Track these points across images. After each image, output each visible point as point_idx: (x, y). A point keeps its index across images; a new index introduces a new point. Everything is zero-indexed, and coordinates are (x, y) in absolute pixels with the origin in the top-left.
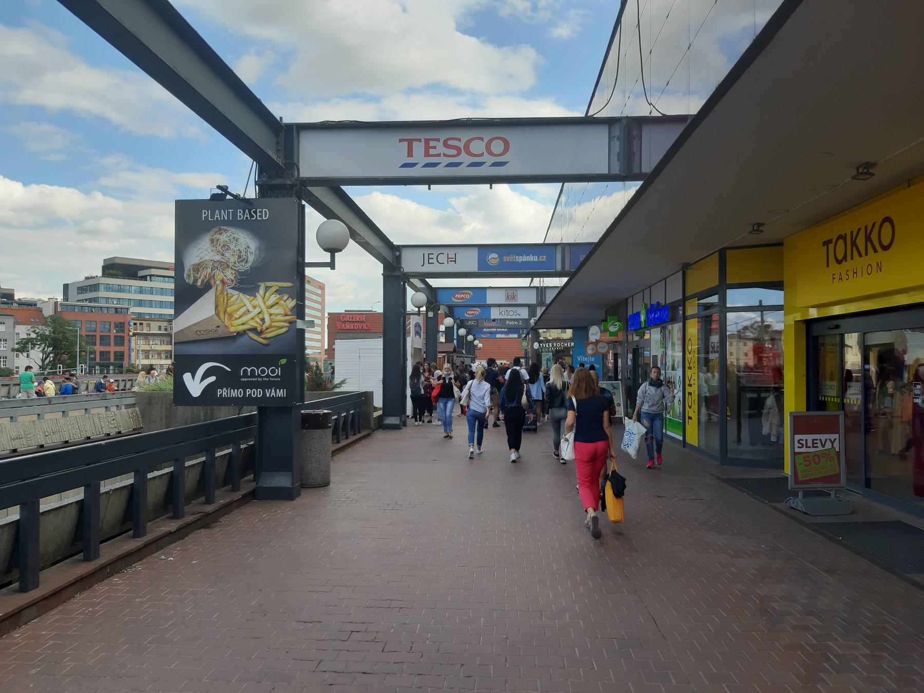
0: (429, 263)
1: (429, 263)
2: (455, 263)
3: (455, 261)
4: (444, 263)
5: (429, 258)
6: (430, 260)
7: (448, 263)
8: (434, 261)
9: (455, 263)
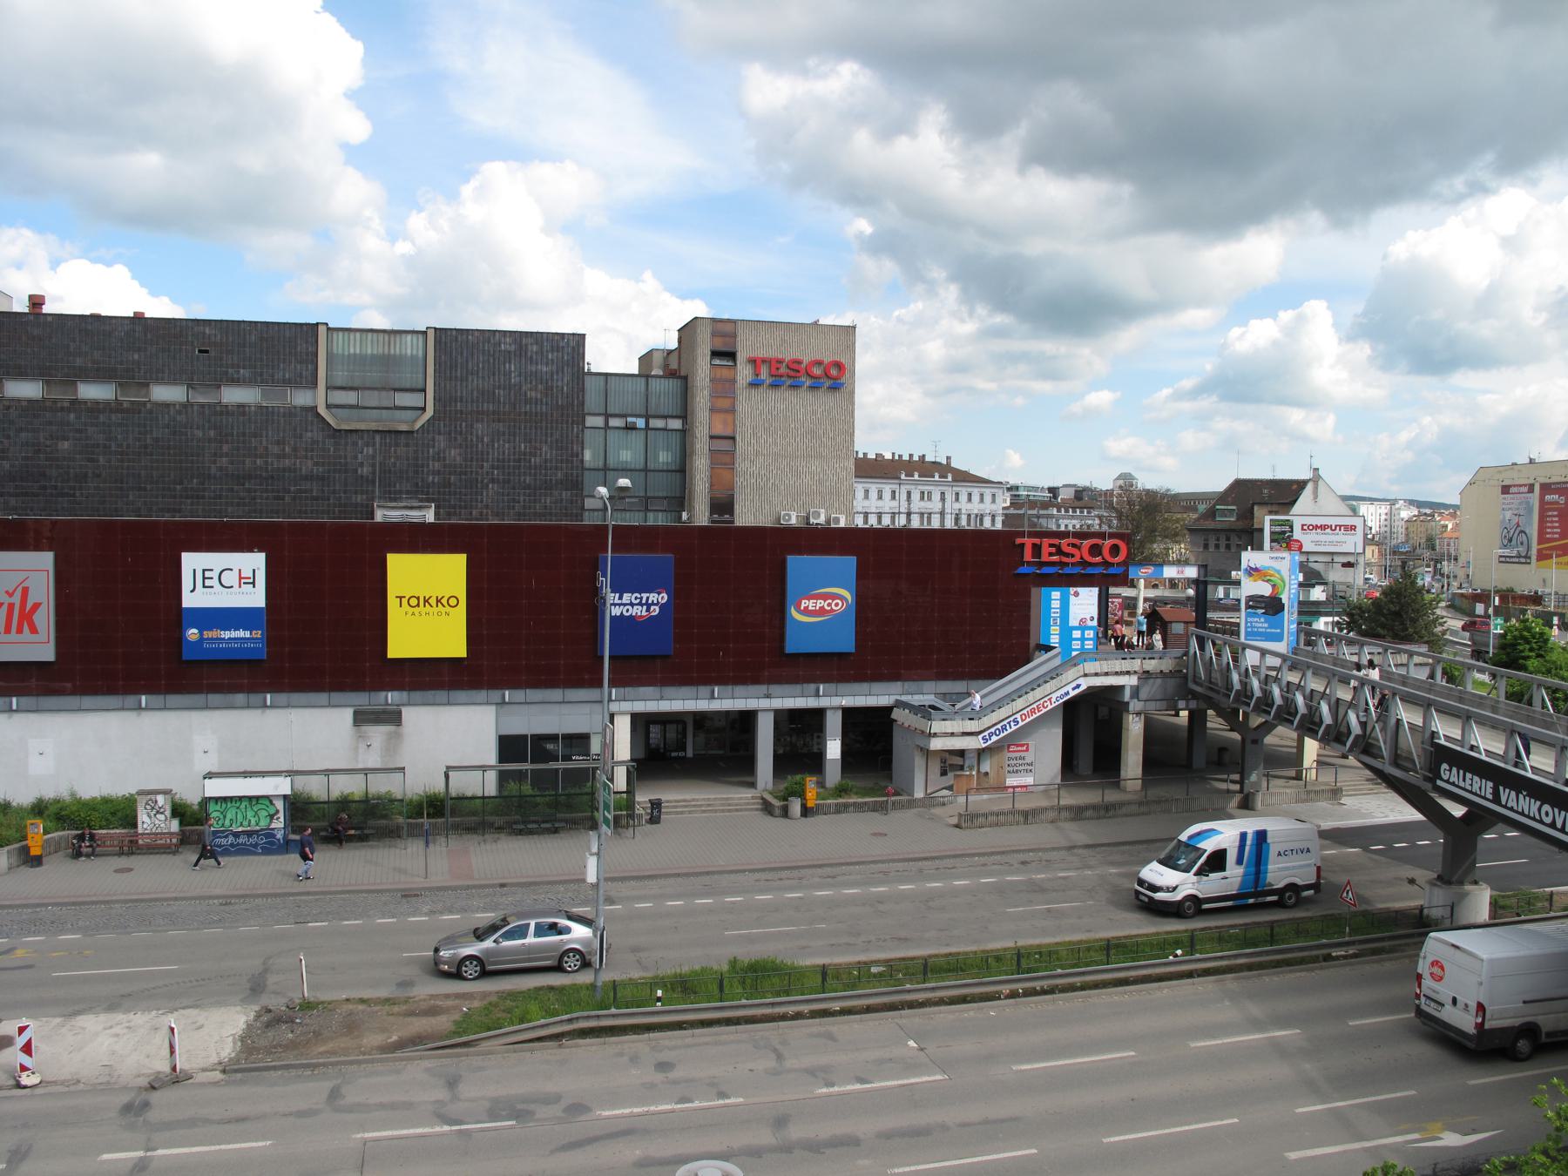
0: (204, 586)
1: (204, 586)
2: (254, 587)
3: (253, 583)
4: (232, 587)
5: (204, 578)
6: (206, 581)
7: (240, 586)
8: (215, 582)
9: (254, 587)
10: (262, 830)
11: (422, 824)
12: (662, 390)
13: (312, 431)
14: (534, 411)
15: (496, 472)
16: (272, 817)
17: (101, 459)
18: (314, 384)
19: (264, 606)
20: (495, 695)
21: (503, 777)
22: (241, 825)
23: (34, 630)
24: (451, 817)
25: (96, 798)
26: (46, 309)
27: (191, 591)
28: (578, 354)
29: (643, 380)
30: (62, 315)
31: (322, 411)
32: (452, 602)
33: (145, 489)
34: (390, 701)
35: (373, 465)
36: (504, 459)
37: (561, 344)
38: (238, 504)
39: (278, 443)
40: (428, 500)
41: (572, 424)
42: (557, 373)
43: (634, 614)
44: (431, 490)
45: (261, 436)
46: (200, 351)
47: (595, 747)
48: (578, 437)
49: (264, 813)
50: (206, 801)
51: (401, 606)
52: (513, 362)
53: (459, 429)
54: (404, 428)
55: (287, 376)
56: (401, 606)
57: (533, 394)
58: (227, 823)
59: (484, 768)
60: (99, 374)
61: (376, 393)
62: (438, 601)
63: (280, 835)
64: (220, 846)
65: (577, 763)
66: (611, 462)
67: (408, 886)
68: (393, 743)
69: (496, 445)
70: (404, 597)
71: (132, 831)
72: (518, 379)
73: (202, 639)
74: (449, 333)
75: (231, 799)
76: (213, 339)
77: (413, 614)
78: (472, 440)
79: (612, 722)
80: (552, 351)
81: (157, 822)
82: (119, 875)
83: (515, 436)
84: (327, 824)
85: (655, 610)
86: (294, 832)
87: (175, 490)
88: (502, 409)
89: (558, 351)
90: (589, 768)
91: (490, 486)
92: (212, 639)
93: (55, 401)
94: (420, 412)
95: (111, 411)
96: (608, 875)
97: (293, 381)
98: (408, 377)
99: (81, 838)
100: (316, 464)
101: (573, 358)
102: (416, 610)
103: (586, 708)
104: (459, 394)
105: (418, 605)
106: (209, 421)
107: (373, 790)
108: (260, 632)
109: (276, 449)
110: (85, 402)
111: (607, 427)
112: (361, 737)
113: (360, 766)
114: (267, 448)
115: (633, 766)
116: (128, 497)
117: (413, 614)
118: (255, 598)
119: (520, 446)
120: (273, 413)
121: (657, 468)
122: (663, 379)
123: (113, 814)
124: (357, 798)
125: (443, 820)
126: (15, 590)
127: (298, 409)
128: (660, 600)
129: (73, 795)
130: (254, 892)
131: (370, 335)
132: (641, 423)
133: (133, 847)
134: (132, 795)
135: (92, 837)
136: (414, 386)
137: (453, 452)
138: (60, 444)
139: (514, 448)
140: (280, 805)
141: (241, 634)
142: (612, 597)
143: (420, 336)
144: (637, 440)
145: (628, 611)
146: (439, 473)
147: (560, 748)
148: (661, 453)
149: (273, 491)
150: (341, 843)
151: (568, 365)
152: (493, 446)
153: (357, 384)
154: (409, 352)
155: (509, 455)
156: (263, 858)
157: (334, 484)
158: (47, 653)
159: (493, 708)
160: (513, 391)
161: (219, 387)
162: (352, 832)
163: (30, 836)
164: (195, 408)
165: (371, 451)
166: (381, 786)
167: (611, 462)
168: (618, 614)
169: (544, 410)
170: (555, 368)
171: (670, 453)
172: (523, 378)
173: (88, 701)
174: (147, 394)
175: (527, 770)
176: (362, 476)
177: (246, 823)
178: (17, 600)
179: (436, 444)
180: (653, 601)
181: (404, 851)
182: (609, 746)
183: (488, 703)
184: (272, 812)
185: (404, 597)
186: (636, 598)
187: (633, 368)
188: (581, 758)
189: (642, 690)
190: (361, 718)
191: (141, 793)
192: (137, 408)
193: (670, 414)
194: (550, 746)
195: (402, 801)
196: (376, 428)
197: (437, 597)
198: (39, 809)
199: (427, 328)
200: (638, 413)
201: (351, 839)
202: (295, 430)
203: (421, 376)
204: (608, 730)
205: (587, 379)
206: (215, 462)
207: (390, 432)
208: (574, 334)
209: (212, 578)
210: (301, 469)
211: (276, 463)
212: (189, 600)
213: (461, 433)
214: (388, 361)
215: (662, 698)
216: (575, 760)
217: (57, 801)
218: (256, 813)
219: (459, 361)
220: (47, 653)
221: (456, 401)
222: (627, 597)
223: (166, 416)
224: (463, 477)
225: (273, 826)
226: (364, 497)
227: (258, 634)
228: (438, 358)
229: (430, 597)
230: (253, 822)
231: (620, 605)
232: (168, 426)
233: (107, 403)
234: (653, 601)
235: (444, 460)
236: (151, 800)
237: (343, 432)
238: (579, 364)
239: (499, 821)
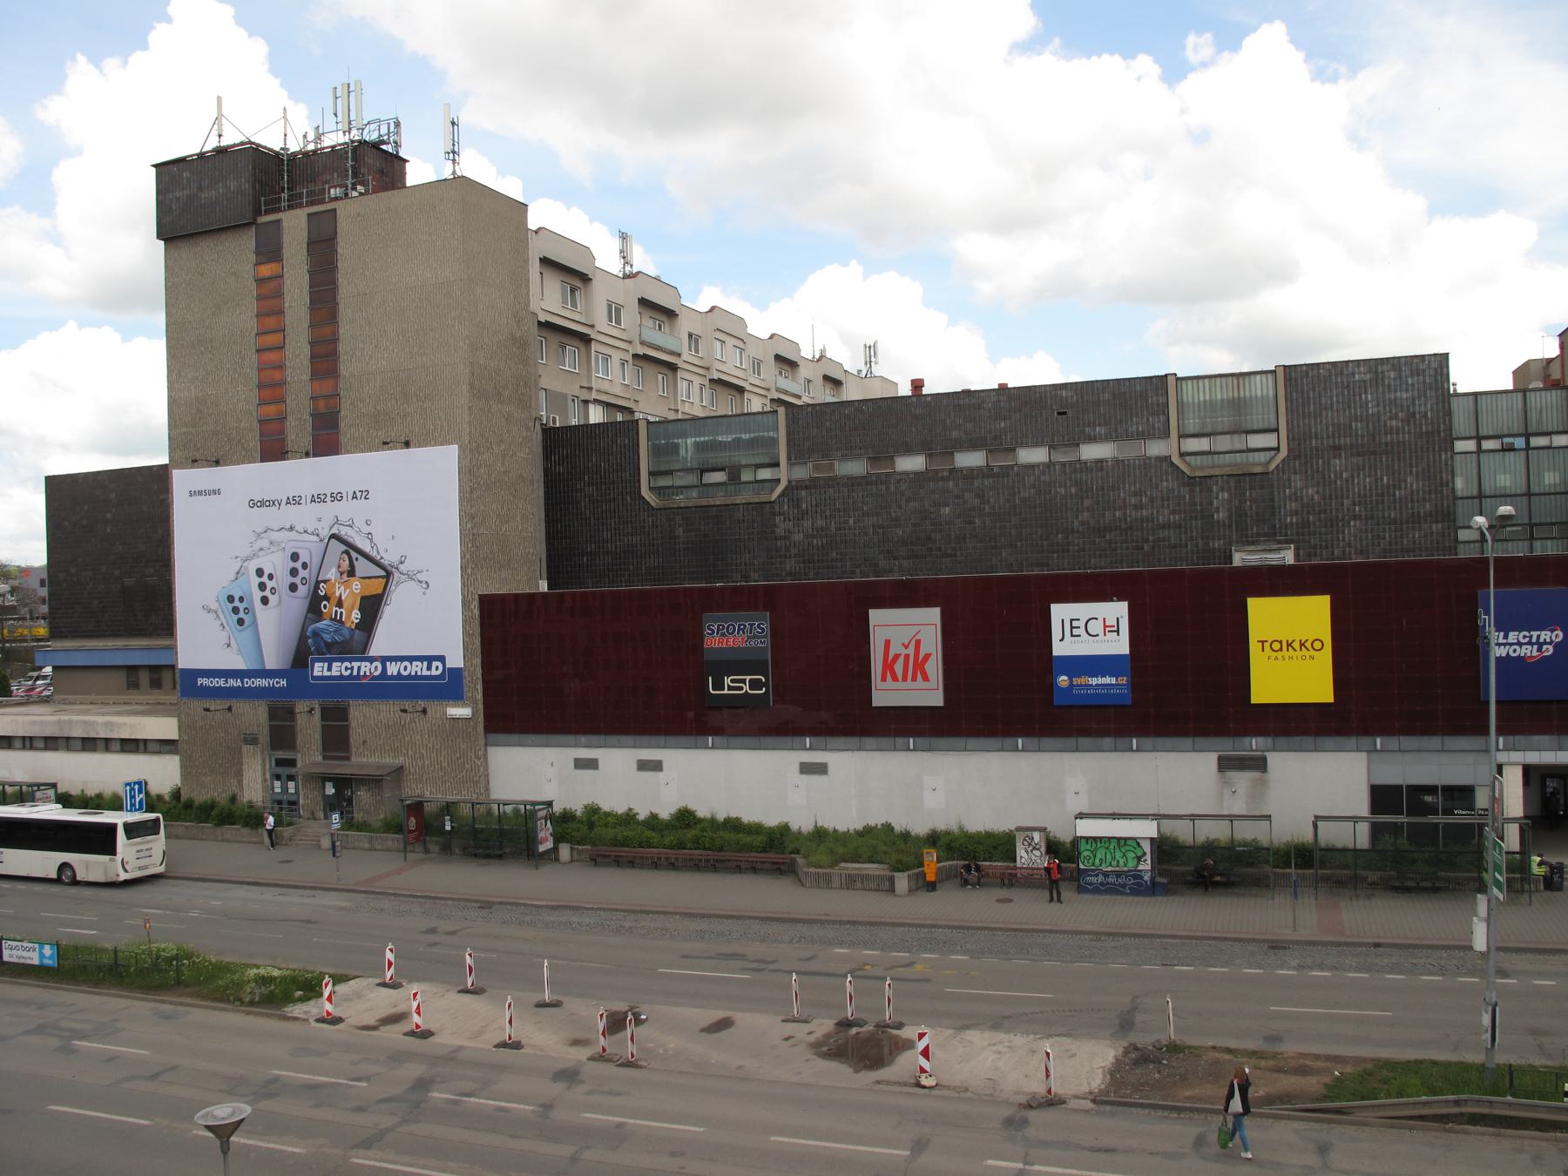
0: (1072, 635)
1: (1072, 635)
2: (1118, 635)
3: (1118, 631)
5: (1072, 628)
6: (1074, 630)
7: (1105, 635)
8: (1082, 631)
9: (1118, 635)
10: (1130, 871)
11: (1290, 875)
12: (1544, 405)
13: (1167, 481)
14: (1395, 440)
15: (1357, 508)
16: (1139, 859)
17: (977, 521)
18: (1166, 434)
19: (1128, 653)
20: (1365, 741)
21: (1377, 830)
22: (1110, 865)
23: (926, 678)
24: (1321, 868)
25: (981, 832)
26: (925, 391)
27: (1061, 640)
28: (1442, 375)
29: (1520, 395)
30: (939, 394)
31: (1176, 460)
32: (1317, 645)
33: (1016, 546)
34: (1254, 747)
35: (1229, 510)
36: (1365, 495)
37: (1421, 367)
38: (1101, 556)
39: (1135, 494)
40: (1287, 542)
41: (1440, 450)
42: (1419, 398)
43: (1522, 655)
44: (1289, 533)
45: (1119, 490)
46: (1059, 414)
47: (1482, 800)
48: (1447, 464)
49: (1131, 855)
50: (1076, 841)
51: (1263, 650)
52: (1369, 391)
53: (1315, 467)
54: (1258, 470)
55: (1140, 429)
56: (1263, 650)
57: (1394, 423)
58: (1097, 862)
59: (1355, 819)
60: (973, 446)
61: (1228, 436)
62: (1302, 645)
63: (1147, 877)
64: (1091, 884)
65: (1461, 817)
66: (1487, 490)
67: (1275, 938)
68: (1259, 791)
69: (1356, 481)
70: (1266, 641)
71: (1012, 865)
72: (1376, 409)
73: (1071, 686)
74: (1299, 369)
75: (1101, 838)
76: (1069, 400)
77: (1276, 658)
78: (1330, 477)
79: (1500, 773)
80: (1412, 375)
81: (1033, 857)
82: (1001, 905)
83: (1376, 469)
84: (1192, 868)
85: (1549, 650)
86: (1161, 875)
87: (1042, 545)
88: (1360, 442)
89: (1418, 375)
90: (1475, 823)
91: (1352, 523)
92: (1081, 685)
93: (936, 472)
94: (1273, 453)
95: (984, 477)
96: (1499, 945)
97: (1146, 434)
98: (1257, 420)
99: (968, 868)
100: (1174, 512)
101: (1436, 381)
102: (1279, 654)
103: (1470, 758)
104: (1313, 430)
105: (1281, 649)
106: (1070, 479)
107: (1239, 836)
108: (1125, 678)
109: (1133, 501)
110: (961, 470)
111: (1479, 450)
112: (1226, 783)
113: (1225, 812)
114: (1125, 500)
115: (1528, 824)
116: (1001, 554)
117: (1276, 658)
118: (1120, 645)
119: (1382, 480)
120: (1129, 465)
121: (1542, 491)
122: (1543, 393)
123: (995, 848)
124: (1222, 844)
125: (1311, 871)
126: (910, 642)
127: (1153, 460)
128: (1554, 638)
129: (961, 828)
130: (1123, 931)
131: (1218, 380)
132: (1519, 443)
133: (1012, 880)
134: (1011, 831)
135: (978, 869)
136: (1266, 426)
137: (1310, 491)
138: (942, 511)
139: (1376, 482)
140: (1147, 847)
141: (1108, 680)
142: (1495, 636)
143: (1270, 376)
144: (1515, 461)
145: (1515, 651)
146: (1296, 513)
147: (1440, 800)
148: (1546, 474)
149: (1132, 541)
150: (1206, 889)
151: (1431, 388)
152: (1354, 480)
153: (1208, 429)
154: (1259, 393)
155: (1371, 489)
156: (1130, 898)
157: (1192, 532)
158: (936, 698)
159: (1365, 754)
160: (1371, 424)
161: (1078, 445)
162: (1218, 878)
163: (926, 863)
164: (1057, 467)
165: (1226, 495)
166: (1247, 832)
167: (1488, 489)
168: (1504, 655)
169: (1407, 439)
170: (1416, 393)
171: (1557, 474)
172: (1381, 409)
173: (972, 742)
174: (1015, 458)
175: (1403, 823)
176: (1218, 522)
177: (1114, 863)
178: (911, 650)
179: (1293, 484)
180: (1545, 640)
181: (1271, 901)
182: (1496, 800)
183: (1358, 750)
184: (1140, 854)
185: (1266, 641)
186: (1524, 637)
187: (1507, 384)
188: (1464, 813)
189: (1536, 738)
190: (1225, 764)
191: (1019, 829)
192: (1006, 470)
193: (1555, 429)
194: (1429, 799)
195: (1268, 849)
196: (1230, 473)
197: (1301, 641)
198: (934, 839)
199: (1276, 367)
200: (1516, 432)
201: (1217, 884)
202: (1151, 480)
203: (1273, 416)
204: (1496, 783)
205: (1454, 401)
206: (1077, 518)
207: (1243, 475)
208: (1435, 355)
209: (1079, 627)
210: (1158, 518)
211: (1133, 513)
212: (1060, 648)
213: (1318, 471)
214: (1238, 405)
215: (1560, 749)
216: (1458, 815)
217: (948, 833)
218: (1124, 853)
219: (1312, 396)
220: (936, 698)
221: (1310, 439)
222: (1512, 636)
223: (1032, 478)
224: (1323, 516)
225: (1140, 868)
226: (1222, 542)
227: (1124, 680)
228: (1289, 395)
229: (1294, 641)
230: (1121, 863)
231: (1505, 645)
232: (1033, 486)
233: (980, 469)
234: (1545, 640)
235: (1302, 500)
236: (1028, 836)
237: (1197, 479)
238: (1443, 388)
239: (1373, 876)
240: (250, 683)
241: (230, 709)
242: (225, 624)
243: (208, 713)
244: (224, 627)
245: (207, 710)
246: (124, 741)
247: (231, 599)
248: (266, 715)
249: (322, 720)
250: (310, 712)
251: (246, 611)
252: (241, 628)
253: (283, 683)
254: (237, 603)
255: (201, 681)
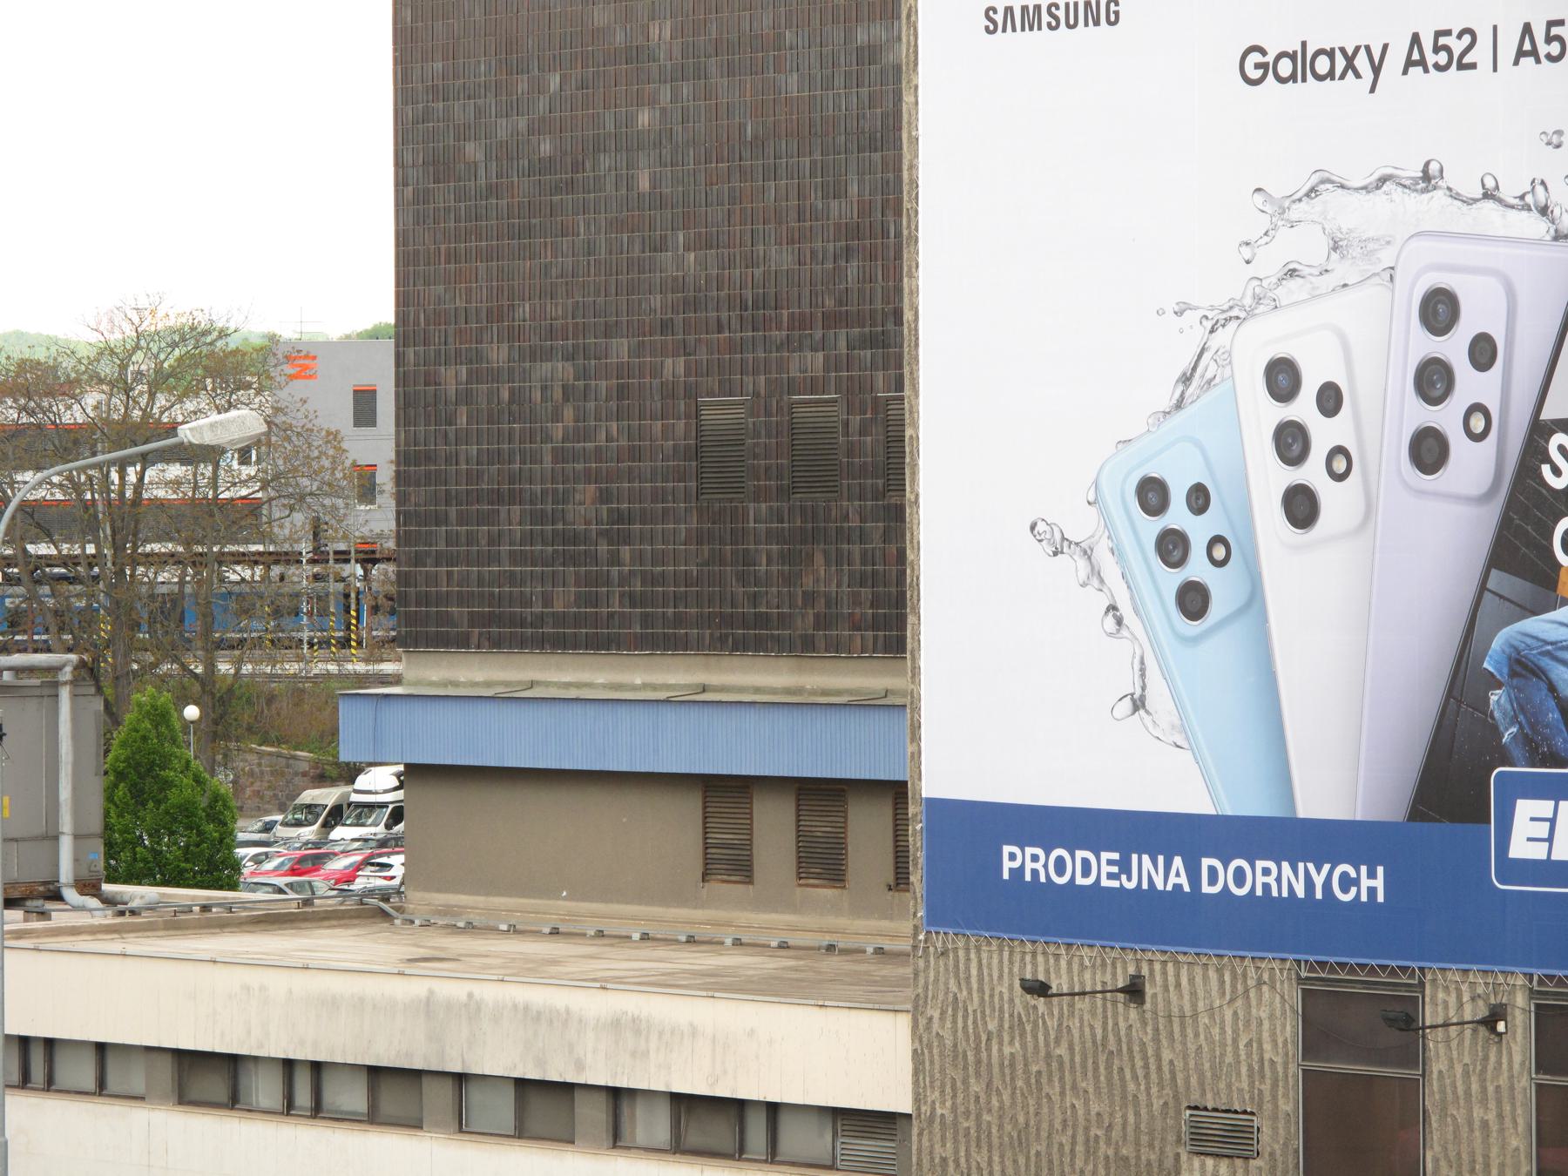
240: (1226, 877)
241: (1134, 991)
242: (1126, 610)
243: (1041, 1002)
244: (1119, 622)
245: (1039, 989)
246: (682, 1103)
247: (1152, 494)
248: (1290, 1029)
249: (1541, 1067)
250: (1490, 1022)
251: (1219, 552)
252: (1194, 627)
253: (1373, 883)
254: (1178, 515)
255: (1020, 859)
